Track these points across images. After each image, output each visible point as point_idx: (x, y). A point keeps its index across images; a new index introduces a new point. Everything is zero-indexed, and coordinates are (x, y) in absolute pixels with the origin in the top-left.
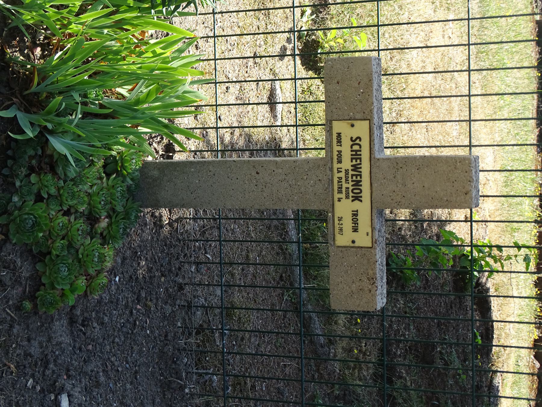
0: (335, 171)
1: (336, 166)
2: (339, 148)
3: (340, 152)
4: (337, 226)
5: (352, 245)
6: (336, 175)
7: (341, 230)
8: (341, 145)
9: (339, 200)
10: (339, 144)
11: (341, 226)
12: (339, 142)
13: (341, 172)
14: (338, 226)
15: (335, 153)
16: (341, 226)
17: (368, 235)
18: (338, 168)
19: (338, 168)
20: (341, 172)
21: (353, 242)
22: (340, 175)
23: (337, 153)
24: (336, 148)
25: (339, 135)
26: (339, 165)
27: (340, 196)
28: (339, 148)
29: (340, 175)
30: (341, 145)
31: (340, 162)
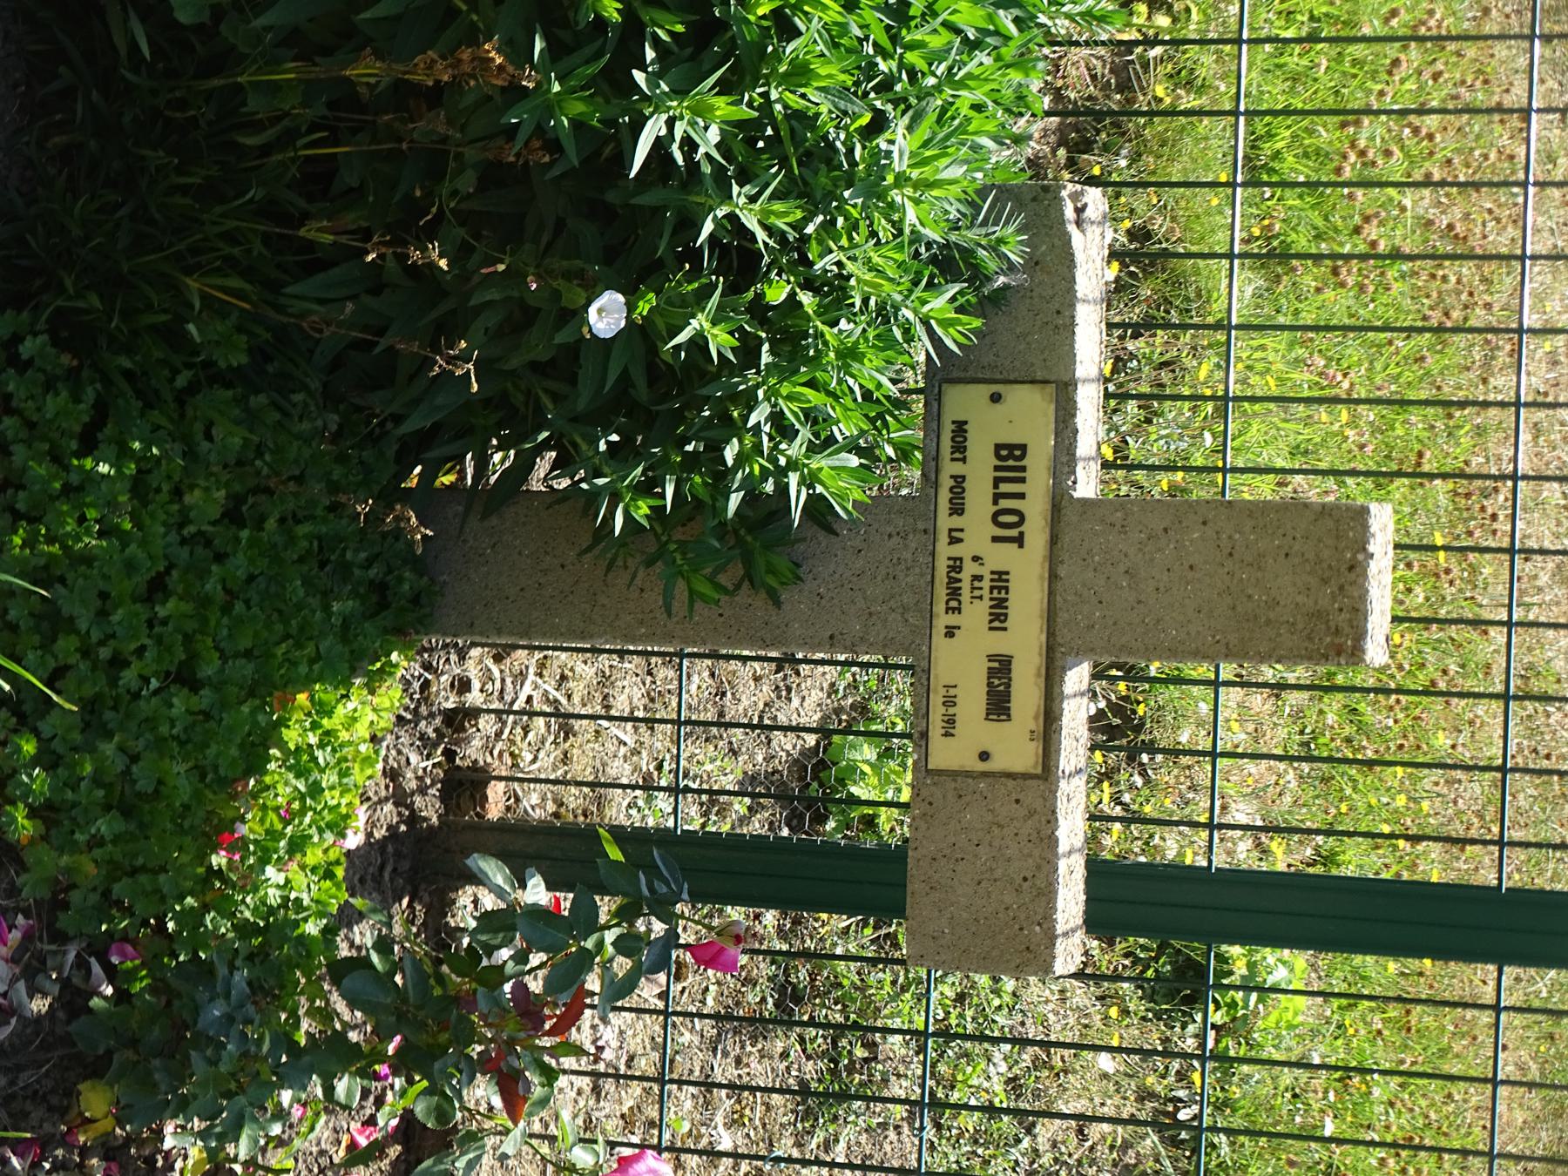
0: (943, 538)
1: (945, 521)
2: (958, 468)
3: (959, 480)
4: (937, 712)
6: (944, 551)
7: (950, 721)
8: (964, 460)
10: (957, 455)
11: (951, 711)
12: (960, 448)
13: (961, 540)
14: (943, 710)
15: (946, 483)
16: (951, 711)
18: (951, 530)
19: (951, 530)
20: (961, 540)
21: (984, 756)
22: (956, 550)
23: (952, 483)
24: (950, 468)
25: (960, 428)
26: (956, 521)
28: (958, 468)
29: (956, 550)
30: (964, 460)
31: (957, 509)
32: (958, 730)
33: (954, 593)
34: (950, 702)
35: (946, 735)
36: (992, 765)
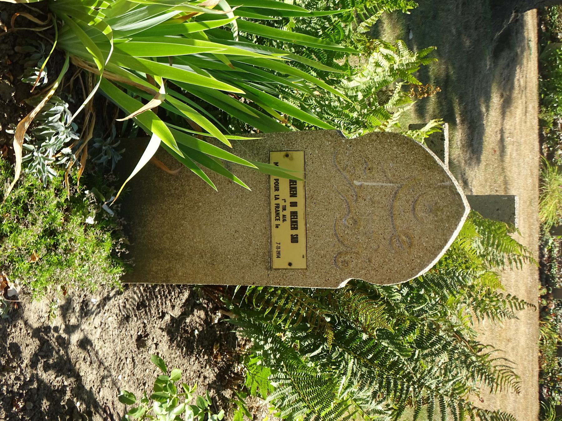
1: (273, 193)
4: (275, 250)
5: (289, 267)
7: (279, 253)
9: (277, 226)
11: (279, 250)
13: (278, 199)
16: (279, 250)
17: (303, 257)
20: (278, 199)
21: (290, 264)
22: (277, 202)
26: (277, 193)
27: (278, 222)
29: (277, 202)
31: (277, 189)
32: (282, 255)
33: (277, 214)
34: (278, 248)
35: (278, 257)
36: (292, 267)
